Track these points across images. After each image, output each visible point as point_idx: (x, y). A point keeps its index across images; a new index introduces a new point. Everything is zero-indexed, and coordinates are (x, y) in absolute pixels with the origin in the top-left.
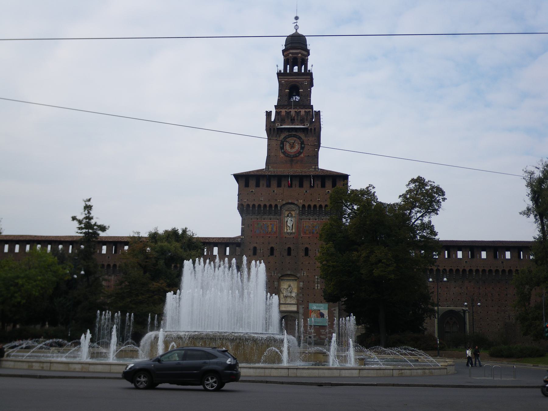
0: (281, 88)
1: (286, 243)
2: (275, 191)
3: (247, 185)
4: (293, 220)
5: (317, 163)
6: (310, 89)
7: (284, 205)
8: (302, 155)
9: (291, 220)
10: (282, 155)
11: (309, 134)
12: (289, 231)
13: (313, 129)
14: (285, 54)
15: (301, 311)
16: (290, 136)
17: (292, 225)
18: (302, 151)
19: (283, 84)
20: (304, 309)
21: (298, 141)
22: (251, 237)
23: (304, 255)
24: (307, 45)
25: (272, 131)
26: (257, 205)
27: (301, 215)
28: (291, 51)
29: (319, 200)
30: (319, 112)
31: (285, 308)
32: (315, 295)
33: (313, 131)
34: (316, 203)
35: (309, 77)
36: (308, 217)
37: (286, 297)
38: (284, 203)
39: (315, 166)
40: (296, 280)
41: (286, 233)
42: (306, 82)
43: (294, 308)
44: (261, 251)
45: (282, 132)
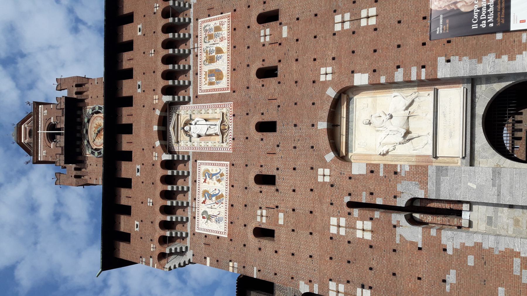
0: (50, 157)
1: (247, 138)
2: (138, 167)
4: (196, 120)
9: (196, 124)
11: (83, 98)
12: (217, 129)
13: (76, 88)
17: (206, 120)
20: (452, 58)
22: (231, 240)
23: (276, 78)
25: (79, 173)
26: (161, 217)
29: (154, 51)
32: (399, 22)
33: (80, 89)
35: (40, 106)
37: (408, 132)
38: (159, 144)
41: (225, 136)
42: (45, 113)
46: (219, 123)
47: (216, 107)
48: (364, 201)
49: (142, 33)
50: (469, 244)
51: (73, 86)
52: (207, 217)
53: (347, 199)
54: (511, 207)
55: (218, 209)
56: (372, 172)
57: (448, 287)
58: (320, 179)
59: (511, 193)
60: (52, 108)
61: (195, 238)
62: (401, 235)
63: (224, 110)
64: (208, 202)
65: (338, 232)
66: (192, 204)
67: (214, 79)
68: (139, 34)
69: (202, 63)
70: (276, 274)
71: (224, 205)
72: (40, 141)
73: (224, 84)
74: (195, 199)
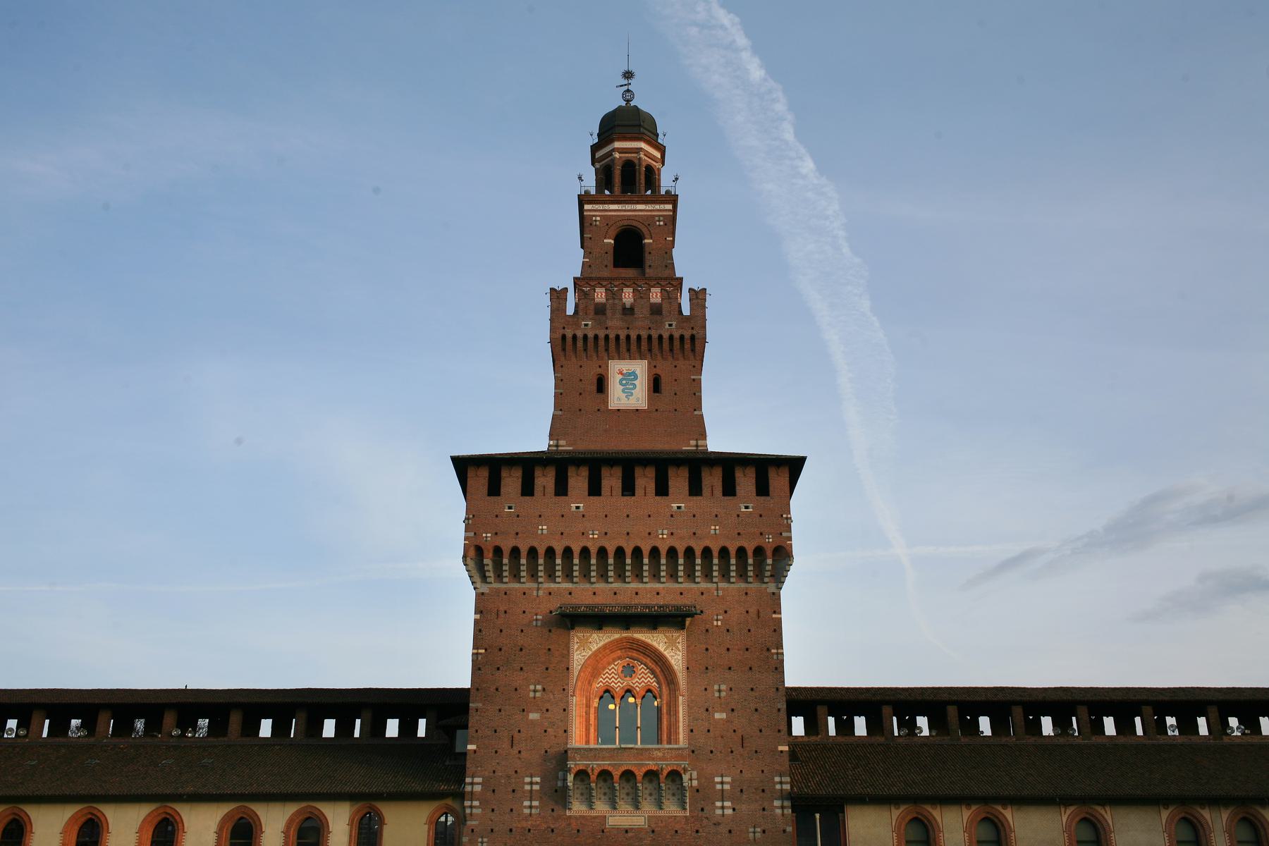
0: (589, 236)
2: (581, 509)
3: (494, 489)
5: (700, 431)
6: (671, 239)
14: (598, 155)
19: (596, 225)
24: (657, 135)
28: (617, 145)
34: (708, 543)
35: (670, 207)
42: (659, 221)
51: (692, 328)
60: (668, 239)
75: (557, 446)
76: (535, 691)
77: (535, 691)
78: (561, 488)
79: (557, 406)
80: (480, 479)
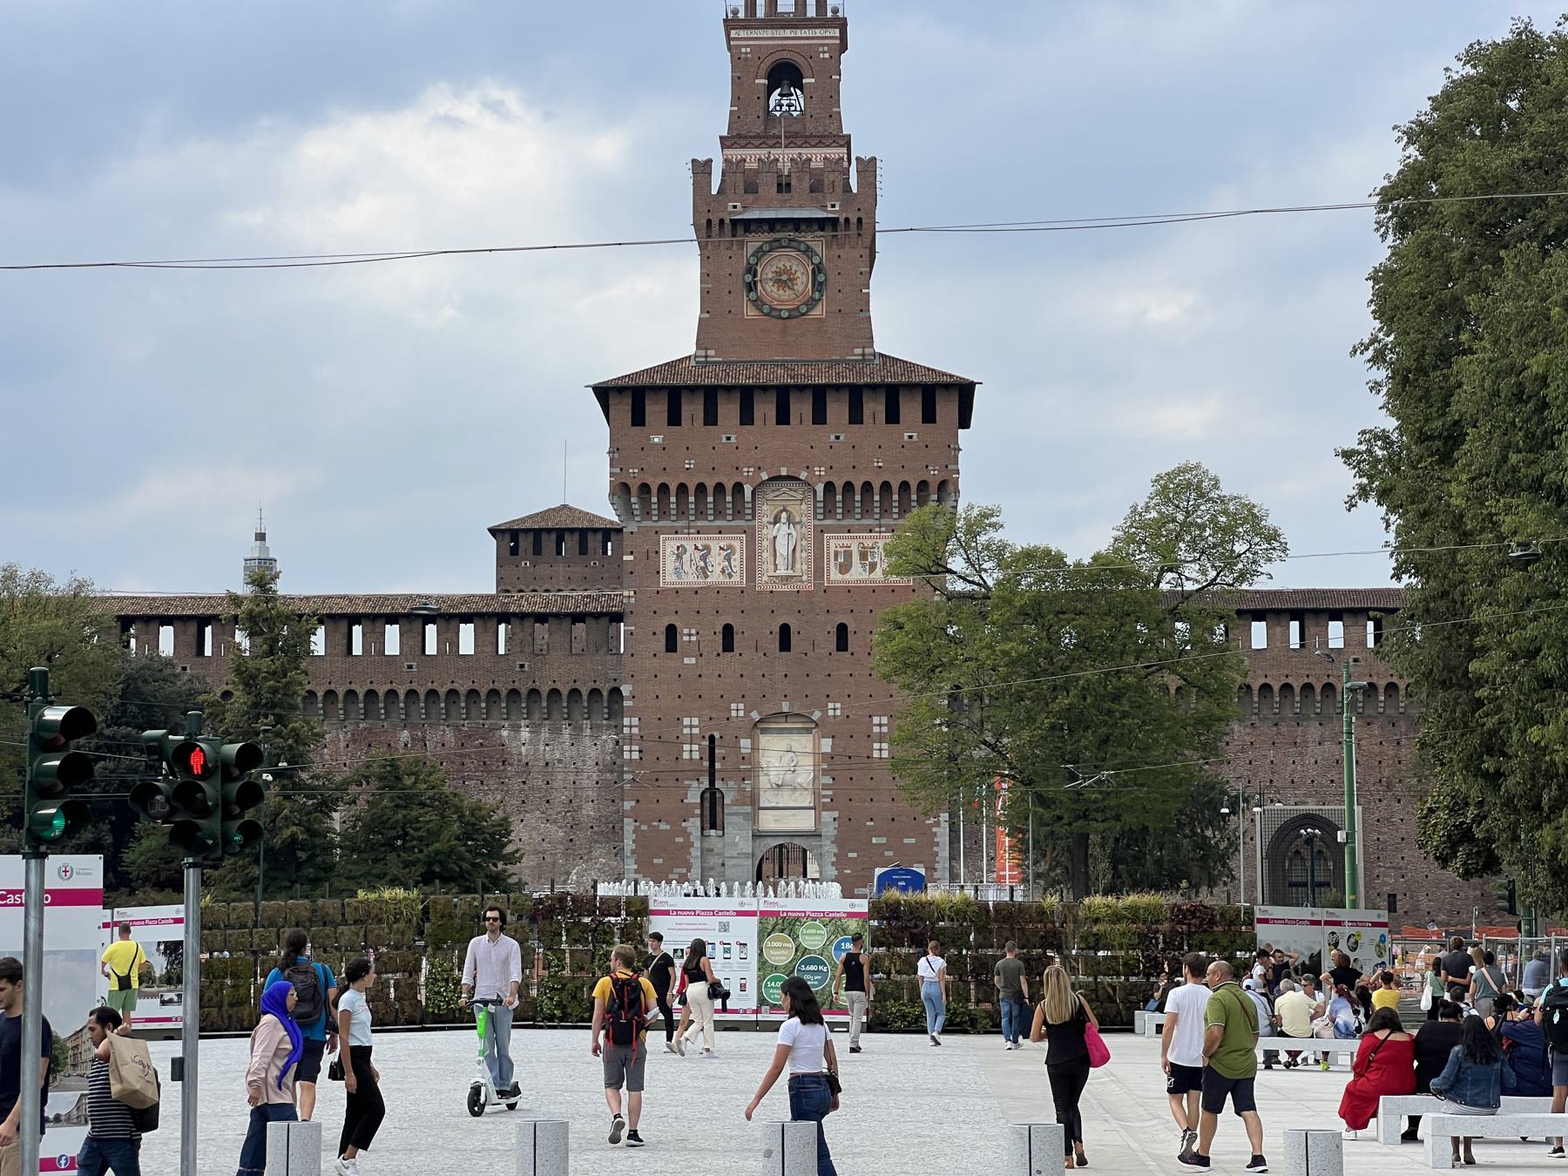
0: (739, 75)
2: (733, 440)
3: (638, 419)
4: (794, 533)
7: (763, 483)
8: (818, 312)
10: (751, 312)
12: (782, 572)
13: (855, 221)
15: (829, 830)
16: (777, 244)
18: (817, 295)
19: (746, 59)
20: (836, 822)
21: (803, 258)
27: (821, 517)
30: (874, 159)
31: (775, 820)
33: (853, 226)
36: (845, 522)
39: (864, 347)
40: (808, 731)
42: (824, 52)
43: (805, 822)
44: (694, 638)
45: (747, 230)
46: (790, 572)
47: (808, 563)
48: (716, 751)
49: (906, 442)
50: (692, 839)
52: (680, 553)
53: (717, 735)
54: (723, 865)
55: (690, 572)
56: (743, 758)
57: (656, 823)
58: (733, 706)
59: (734, 866)
61: (653, 534)
62: (689, 786)
63: (805, 578)
64: (698, 554)
65: (686, 726)
66: (693, 527)
67: (841, 560)
68: (906, 435)
69: (861, 540)
70: (632, 655)
71: (696, 579)
72: (769, 33)
73: (835, 575)
74: (698, 533)
75: (706, 357)
76: (690, 635)
77: (690, 635)
78: (711, 418)
79: (704, 308)
80: (623, 409)
